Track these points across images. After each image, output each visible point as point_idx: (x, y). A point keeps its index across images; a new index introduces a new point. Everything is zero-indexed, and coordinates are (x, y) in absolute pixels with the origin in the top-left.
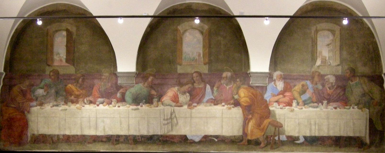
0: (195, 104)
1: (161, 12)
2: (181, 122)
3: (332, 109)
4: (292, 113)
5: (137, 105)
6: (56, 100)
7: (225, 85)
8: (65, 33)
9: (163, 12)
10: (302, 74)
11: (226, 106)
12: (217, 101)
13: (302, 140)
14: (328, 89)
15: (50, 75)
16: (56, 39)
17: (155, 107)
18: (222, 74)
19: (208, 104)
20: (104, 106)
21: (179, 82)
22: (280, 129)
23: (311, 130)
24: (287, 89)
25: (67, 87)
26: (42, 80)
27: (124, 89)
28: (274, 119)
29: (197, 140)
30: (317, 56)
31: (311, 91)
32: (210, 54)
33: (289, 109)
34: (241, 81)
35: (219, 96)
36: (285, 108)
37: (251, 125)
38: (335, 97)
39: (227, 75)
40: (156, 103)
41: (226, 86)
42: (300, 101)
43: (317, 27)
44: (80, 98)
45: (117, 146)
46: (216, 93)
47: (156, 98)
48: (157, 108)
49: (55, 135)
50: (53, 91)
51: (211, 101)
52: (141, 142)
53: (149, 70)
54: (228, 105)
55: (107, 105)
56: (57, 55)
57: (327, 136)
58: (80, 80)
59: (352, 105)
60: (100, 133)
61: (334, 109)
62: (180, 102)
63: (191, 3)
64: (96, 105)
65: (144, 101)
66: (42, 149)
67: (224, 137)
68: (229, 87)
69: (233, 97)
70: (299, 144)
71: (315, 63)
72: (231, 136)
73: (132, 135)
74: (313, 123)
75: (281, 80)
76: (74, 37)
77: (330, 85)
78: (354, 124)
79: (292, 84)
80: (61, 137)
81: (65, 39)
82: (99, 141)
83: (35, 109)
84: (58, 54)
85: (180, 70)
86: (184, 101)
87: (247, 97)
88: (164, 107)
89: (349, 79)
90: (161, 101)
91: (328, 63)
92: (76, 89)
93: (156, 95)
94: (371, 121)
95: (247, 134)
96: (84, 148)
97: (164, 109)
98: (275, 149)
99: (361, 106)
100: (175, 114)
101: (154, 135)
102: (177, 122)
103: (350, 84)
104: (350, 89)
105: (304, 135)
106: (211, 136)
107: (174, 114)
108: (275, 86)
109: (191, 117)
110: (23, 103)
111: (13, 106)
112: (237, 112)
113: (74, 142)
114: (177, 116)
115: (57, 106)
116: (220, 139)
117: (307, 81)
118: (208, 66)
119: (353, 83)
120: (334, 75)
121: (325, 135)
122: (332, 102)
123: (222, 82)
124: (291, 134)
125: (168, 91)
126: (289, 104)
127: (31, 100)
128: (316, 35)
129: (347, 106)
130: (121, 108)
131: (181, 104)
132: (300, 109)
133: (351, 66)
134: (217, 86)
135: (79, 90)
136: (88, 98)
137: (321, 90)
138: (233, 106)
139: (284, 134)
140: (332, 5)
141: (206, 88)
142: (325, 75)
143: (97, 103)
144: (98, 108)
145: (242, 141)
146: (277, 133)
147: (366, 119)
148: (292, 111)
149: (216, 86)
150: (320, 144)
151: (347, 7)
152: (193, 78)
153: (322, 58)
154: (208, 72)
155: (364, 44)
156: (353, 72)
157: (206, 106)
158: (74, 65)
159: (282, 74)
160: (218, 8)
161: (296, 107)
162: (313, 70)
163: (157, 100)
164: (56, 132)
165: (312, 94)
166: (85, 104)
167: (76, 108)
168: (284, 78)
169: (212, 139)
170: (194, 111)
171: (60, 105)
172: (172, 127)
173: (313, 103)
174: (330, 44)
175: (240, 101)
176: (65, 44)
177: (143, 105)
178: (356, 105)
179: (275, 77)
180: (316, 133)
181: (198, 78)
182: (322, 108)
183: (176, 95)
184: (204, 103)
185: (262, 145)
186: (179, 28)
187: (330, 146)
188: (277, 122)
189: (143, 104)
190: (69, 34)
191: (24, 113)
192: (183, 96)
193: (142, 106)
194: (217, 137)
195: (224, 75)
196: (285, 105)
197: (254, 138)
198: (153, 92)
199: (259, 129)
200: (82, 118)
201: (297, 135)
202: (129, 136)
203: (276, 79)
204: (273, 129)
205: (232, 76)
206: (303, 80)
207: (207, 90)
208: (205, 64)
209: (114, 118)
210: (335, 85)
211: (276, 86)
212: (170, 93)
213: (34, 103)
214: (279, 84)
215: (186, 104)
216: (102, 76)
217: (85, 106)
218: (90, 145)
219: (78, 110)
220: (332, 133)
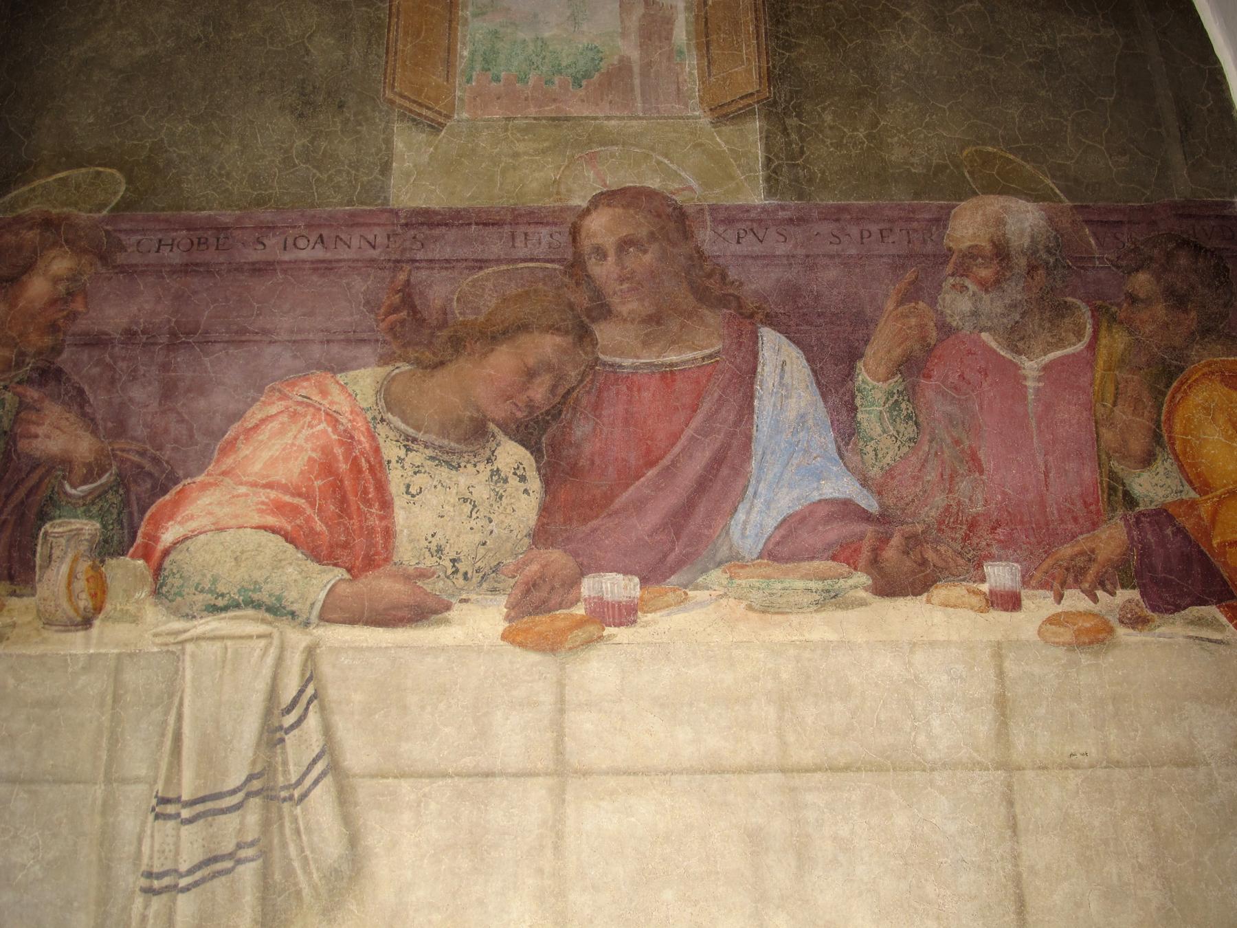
12: (913, 542)
18: (941, 220)
21: (408, 299)
34: (1178, 300)
35: (931, 475)
39: (1000, 222)
40: (72, 576)
47: (87, 506)
48: (76, 644)
51: (836, 532)
54: (1059, 598)
62: (406, 553)
69: (1112, 475)
88: (177, 625)
90: (146, 555)
97: (177, 658)
100: (327, 730)
102: (353, 840)
107: (313, 720)
118: (768, 138)
125: (255, 414)
131: (427, 585)
134: (897, 352)
141: (754, 371)
152: (576, 267)
154: (770, 192)
163: (90, 527)
175: (1208, 535)
183: (355, 463)
184: (734, 561)
192: (444, 472)
207: (765, 405)
208: (724, 114)
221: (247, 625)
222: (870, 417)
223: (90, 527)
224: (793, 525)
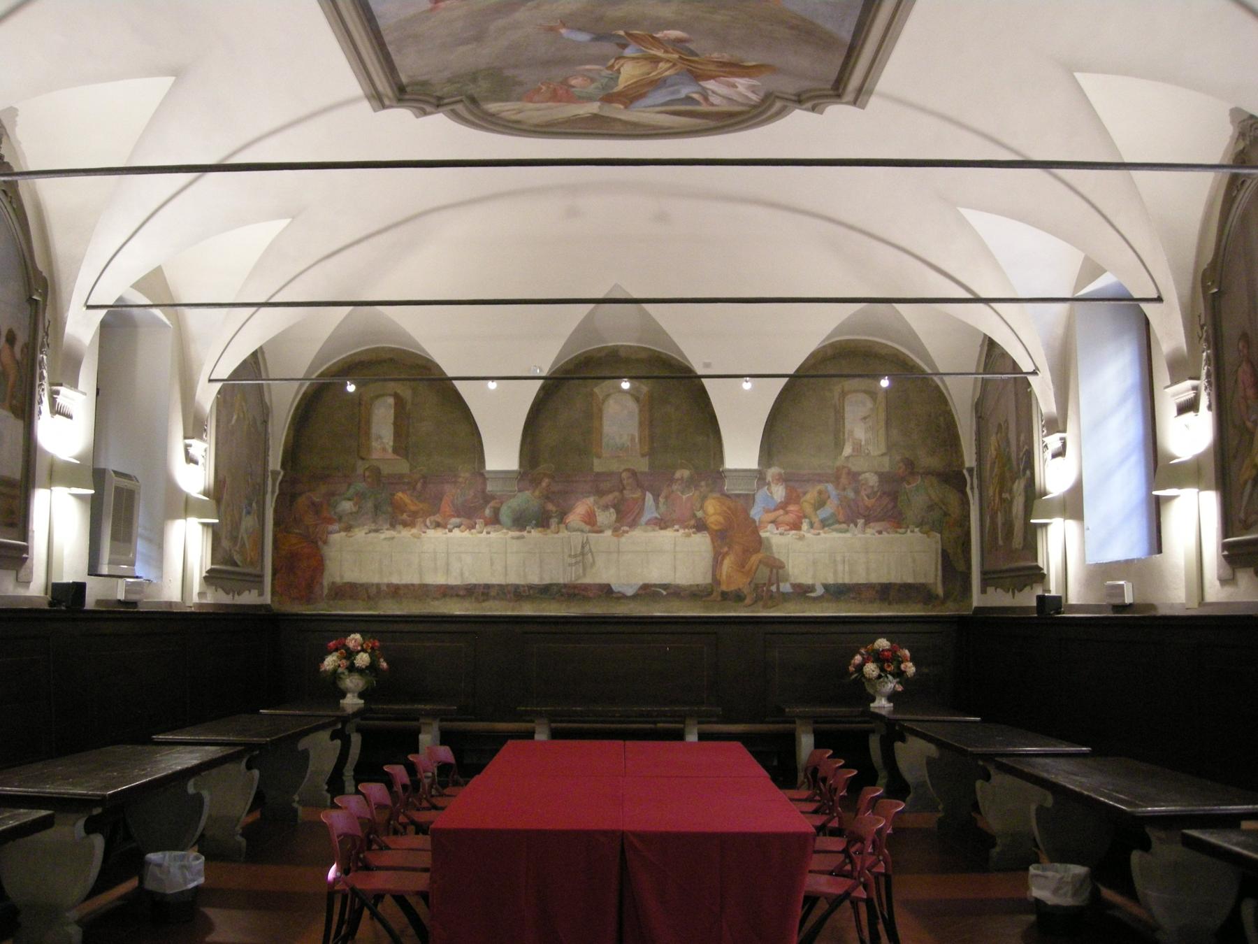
0: (626, 528)
1: (563, 362)
2: (600, 560)
3: (874, 534)
4: (801, 543)
5: (520, 531)
6: (374, 522)
7: (679, 493)
8: (391, 401)
9: (567, 362)
10: (819, 471)
11: (682, 531)
13: (820, 591)
14: (866, 498)
15: (364, 476)
16: (376, 411)
17: (552, 532)
18: (674, 474)
19: (649, 528)
20: (462, 532)
22: (781, 571)
23: (835, 572)
24: (792, 498)
25: (395, 497)
26: (350, 485)
27: (497, 501)
28: (768, 554)
29: (630, 592)
30: (844, 440)
31: (836, 502)
32: (652, 438)
33: (796, 534)
34: (707, 485)
36: (789, 534)
37: (727, 564)
38: (880, 512)
41: (680, 495)
42: (816, 520)
43: (843, 386)
44: (417, 518)
45: (485, 604)
46: (663, 508)
47: (555, 517)
48: (556, 536)
49: (373, 585)
50: (370, 504)
52: (527, 596)
53: (543, 467)
55: (468, 530)
56: (377, 440)
57: (866, 584)
58: (419, 486)
59: (910, 526)
60: (454, 581)
61: (877, 534)
62: (598, 524)
63: (617, 346)
64: (447, 530)
65: (534, 522)
66: (349, 610)
67: (677, 586)
68: (686, 497)
70: (815, 599)
71: (842, 451)
72: (691, 586)
73: (512, 585)
74: (839, 558)
75: (780, 484)
76: (407, 408)
77: (869, 491)
78: (914, 561)
79: (800, 490)
80: (385, 588)
81: (392, 411)
82: (452, 596)
83: (337, 538)
84: (379, 437)
85: (598, 466)
86: (606, 522)
87: (719, 514)
88: (569, 533)
89: (903, 479)
90: (564, 523)
91: (864, 452)
92: (412, 501)
93: (556, 512)
94: (945, 555)
95: (720, 582)
96: (425, 608)
98: (771, 608)
99: (926, 528)
101: (551, 585)
103: (905, 488)
104: (906, 498)
105: (824, 582)
106: (655, 585)
108: (769, 494)
109: (619, 552)
110: (316, 526)
111: (297, 531)
112: (701, 543)
113: (407, 598)
114: (593, 550)
115: (376, 531)
116: (672, 591)
117: (827, 484)
119: (910, 486)
120: (876, 473)
121: (862, 581)
122: (873, 522)
123: (675, 487)
124: (799, 581)
126: (796, 526)
127: (330, 521)
128: (841, 401)
129: (901, 528)
130: (493, 535)
132: (815, 534)
133: (907, 456)
135: (417, 502)
136: (432, 518)
137: (853, 500)
138: (694, 530)
139: (787, 580)
140: (870, 346)
142: (859, 474)
143: (449, 526)
144: (450, 535)
145: (710, 594)
146: (774, 579)
147: (937, 549)
148: (802, 538)
149: (663, 494)
150: (853, 598)
151: (897, 350)
152: (621, 481)
153: (854, 443)
154: (649, 469)
155: (930, 416)
156: (910, 465)
157: (646, 531)
158: (407, 458)
159: (783, 471)
160: (666, 354)
161: (809, 532)
162: (839, 463)
163: (556, 520)
164: (376, 579)
165: (838, 507)
166: (428, 528)
167: (412, 535)
168: (785, 479)
169: (657, 591)
170: (623, 540)
171: (382, 529)
172: (584, 569)
173: (840, 523)
174: (869, 416)
175: (706, 521)
176: (391, 419)
177: (533, 531)
178: (917, 527)
179: (769, 478)
180: (844, 577)
181: (630, 480)
182: (856, 532)
185: (748, 601)
186: (596, 390)
187: (871, 602)
188: (775, 559)
189: (533, 528)
190: (400, 403)
191: (316, 543)
193: (529, 532)
194: (665, 587)
195: (678, 475)
196: (788, 527)
197: (733, 588)
198: (550, 507)
199: (743, 572)
200: (422, 552)
201: (810, 582)
202: (507, 585)
203: (771, 480)
204: (766, 571)
205: (691, 478)
206: (820, 482)
207: (646, 504)
208: (643, 455)
209: (479, 553)
210: (877, 492)
211: (771, 493)
212: (580, 509)
213: (336, 527)
214: (778, 490)
215: (609, 528)
216: (460, 477)
217: (428, 531)
218: (436, 603)
219: (416, 540)
220: (874, 579)
221: (579, 533)
222: (661, 505)
223: (556, 520)
224: (649, 520)
